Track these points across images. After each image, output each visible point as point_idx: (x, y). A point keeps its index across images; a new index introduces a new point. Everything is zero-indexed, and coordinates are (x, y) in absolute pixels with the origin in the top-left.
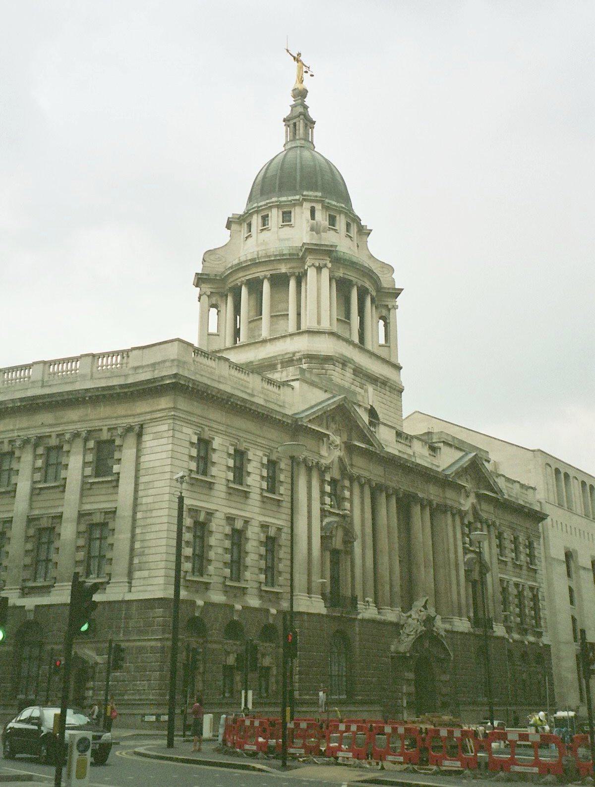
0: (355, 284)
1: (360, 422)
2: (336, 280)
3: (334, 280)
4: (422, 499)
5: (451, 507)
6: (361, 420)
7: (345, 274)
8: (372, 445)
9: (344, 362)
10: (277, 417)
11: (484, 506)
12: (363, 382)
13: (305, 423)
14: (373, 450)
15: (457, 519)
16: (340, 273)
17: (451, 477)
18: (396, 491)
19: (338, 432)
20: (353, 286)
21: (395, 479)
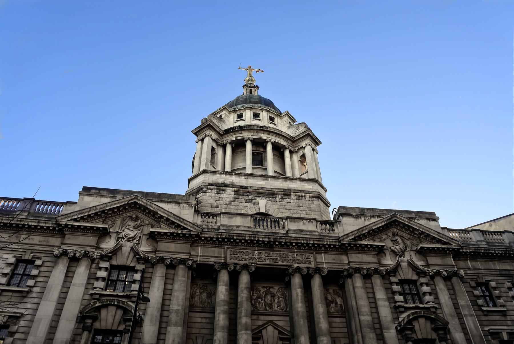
0: (248, 140)
1: (163, 212)
2: (230, 143)
3: (228, 144)
4: (298, 270)
5: (358, 270)
6: (162, 210)
7: (237, 137)
8: (185, 229)
9: (220, 187)
10: (30, 224)
11: (432, 260)
12: (250, 198)
13: (64, 221)
14: (184, 232)
15: (377, 281)
16: (233, 137)
17: (346, 240)
18: (245, 267)
19: (136, 227)
20: (246, 141)
21: (247, 257)
